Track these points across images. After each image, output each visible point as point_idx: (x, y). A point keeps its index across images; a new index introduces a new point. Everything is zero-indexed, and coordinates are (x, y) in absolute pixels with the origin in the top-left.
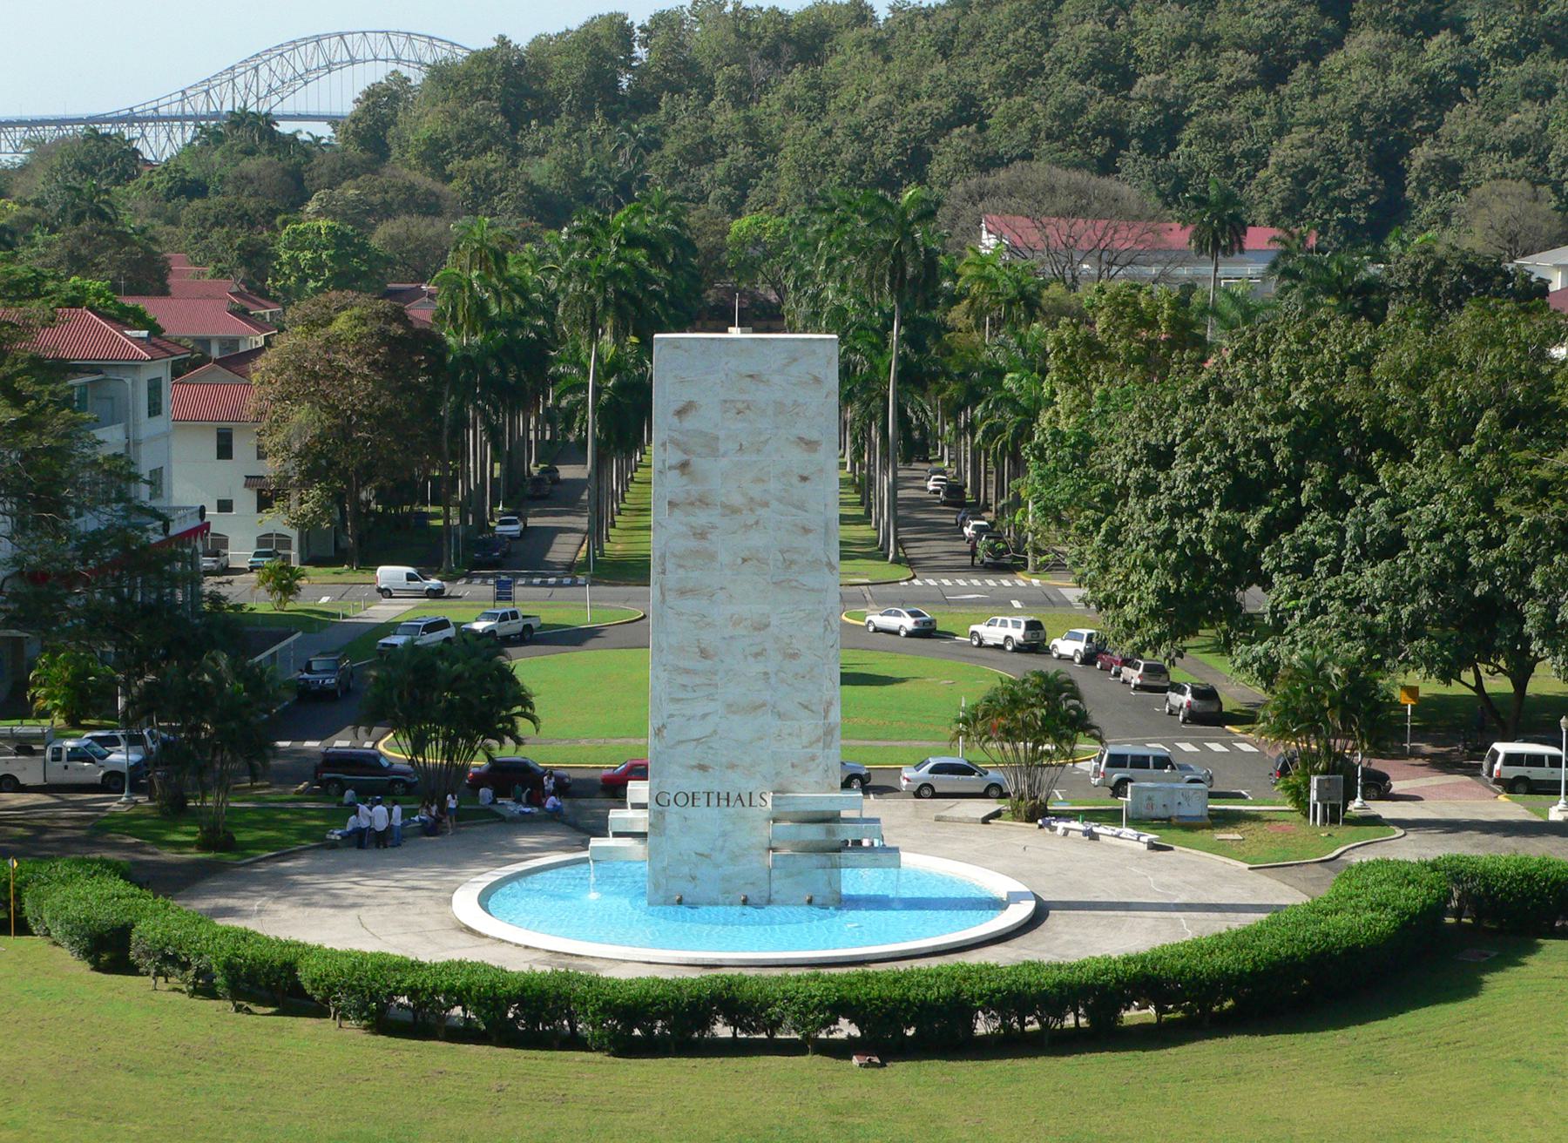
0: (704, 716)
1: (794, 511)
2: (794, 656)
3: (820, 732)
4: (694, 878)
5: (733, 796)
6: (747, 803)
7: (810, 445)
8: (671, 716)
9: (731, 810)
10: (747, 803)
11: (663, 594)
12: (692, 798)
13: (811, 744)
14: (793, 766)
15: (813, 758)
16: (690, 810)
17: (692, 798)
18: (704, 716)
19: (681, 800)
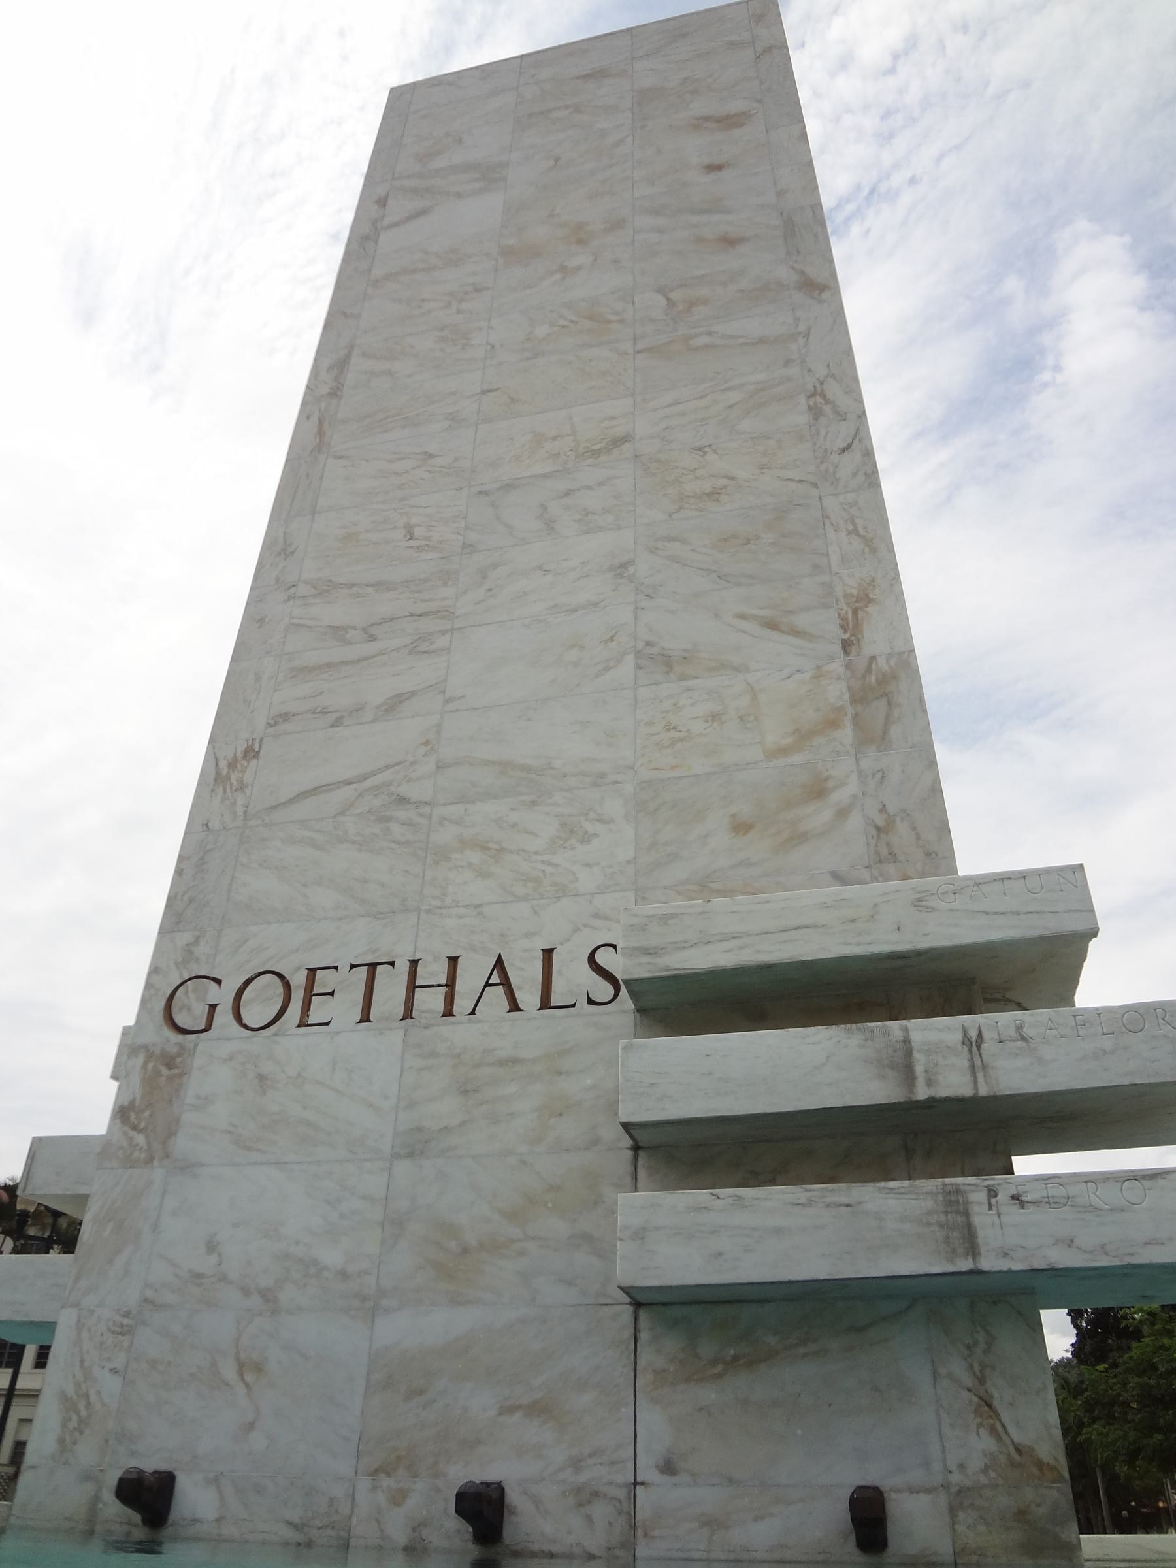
0: (393, 706)
1: (694, 219)
2: (714, 495)
3: (836, 692)
4: (251, 1367)
5: (470, 979)
6: (529, 997)
7: (730, 122)
8: (285, 717)
9: (460, 1033)
10: (529, 997)
11: (321, 432)
13: (803, 737)
14: (741, 827)
15: (818, 790)
16: (291, 1041)
17: (301, 994)
18: (393, 706)
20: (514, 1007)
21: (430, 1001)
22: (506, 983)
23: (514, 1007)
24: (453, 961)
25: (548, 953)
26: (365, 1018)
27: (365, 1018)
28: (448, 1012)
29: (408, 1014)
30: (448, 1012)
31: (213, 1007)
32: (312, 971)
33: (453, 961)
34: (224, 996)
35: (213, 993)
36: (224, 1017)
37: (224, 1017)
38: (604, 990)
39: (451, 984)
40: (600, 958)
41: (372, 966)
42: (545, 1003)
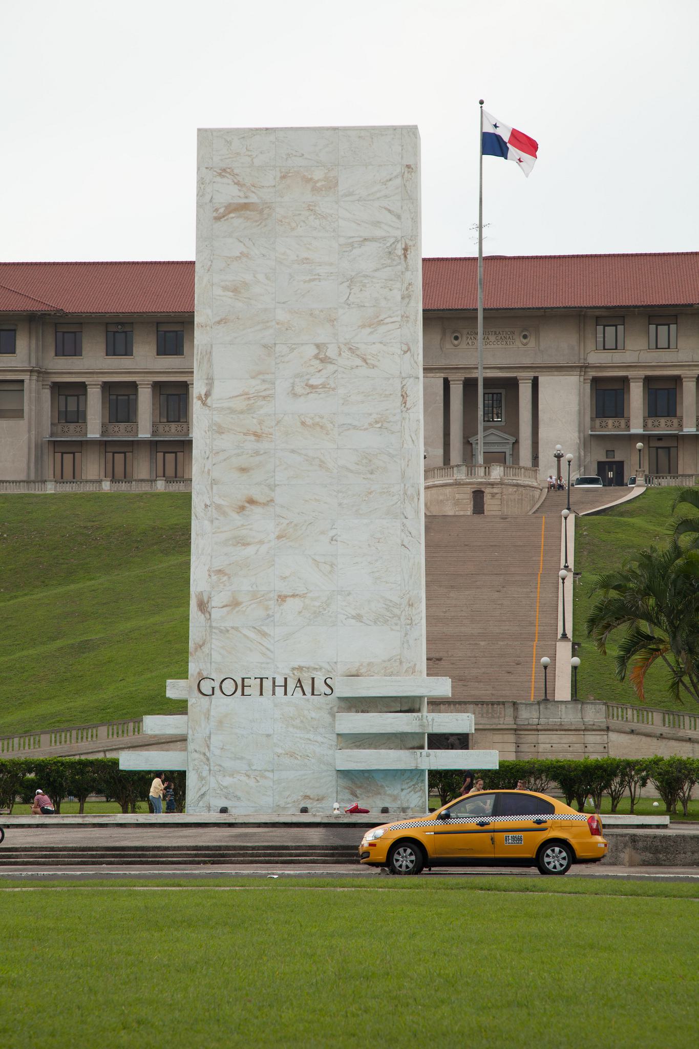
5: (291, 685)
12: (242, 687)
17: (242, 687)
19: (229, 687)
20: (304, 694)
21: (280, 691)
22: (301, 687)
23: (304, 694)
24: (286, 679)
25: (313, 679)
26: (261, 694)
27: (261, 694)
28: (286, 694)
29: (274, 694)
30: (286, 694)
31: (213, 688)
32: (243, 679)
33: (286, 679)
34: (216, 685)
35: (213, 684)
36: (217, 691)
37: (217, 691)
38: (328, 691)
39: (285, 686)
40: (328, 681)
41: (261, 679)
42: (313, 694)
